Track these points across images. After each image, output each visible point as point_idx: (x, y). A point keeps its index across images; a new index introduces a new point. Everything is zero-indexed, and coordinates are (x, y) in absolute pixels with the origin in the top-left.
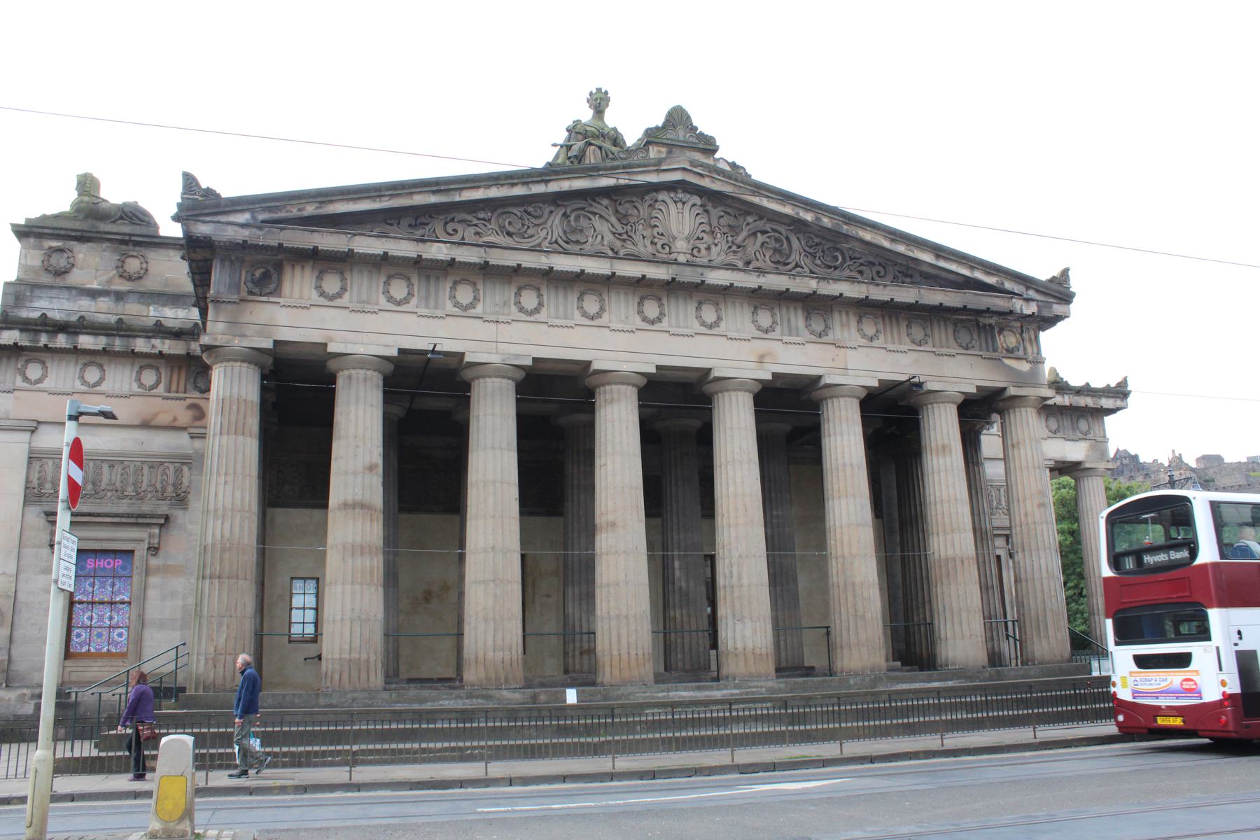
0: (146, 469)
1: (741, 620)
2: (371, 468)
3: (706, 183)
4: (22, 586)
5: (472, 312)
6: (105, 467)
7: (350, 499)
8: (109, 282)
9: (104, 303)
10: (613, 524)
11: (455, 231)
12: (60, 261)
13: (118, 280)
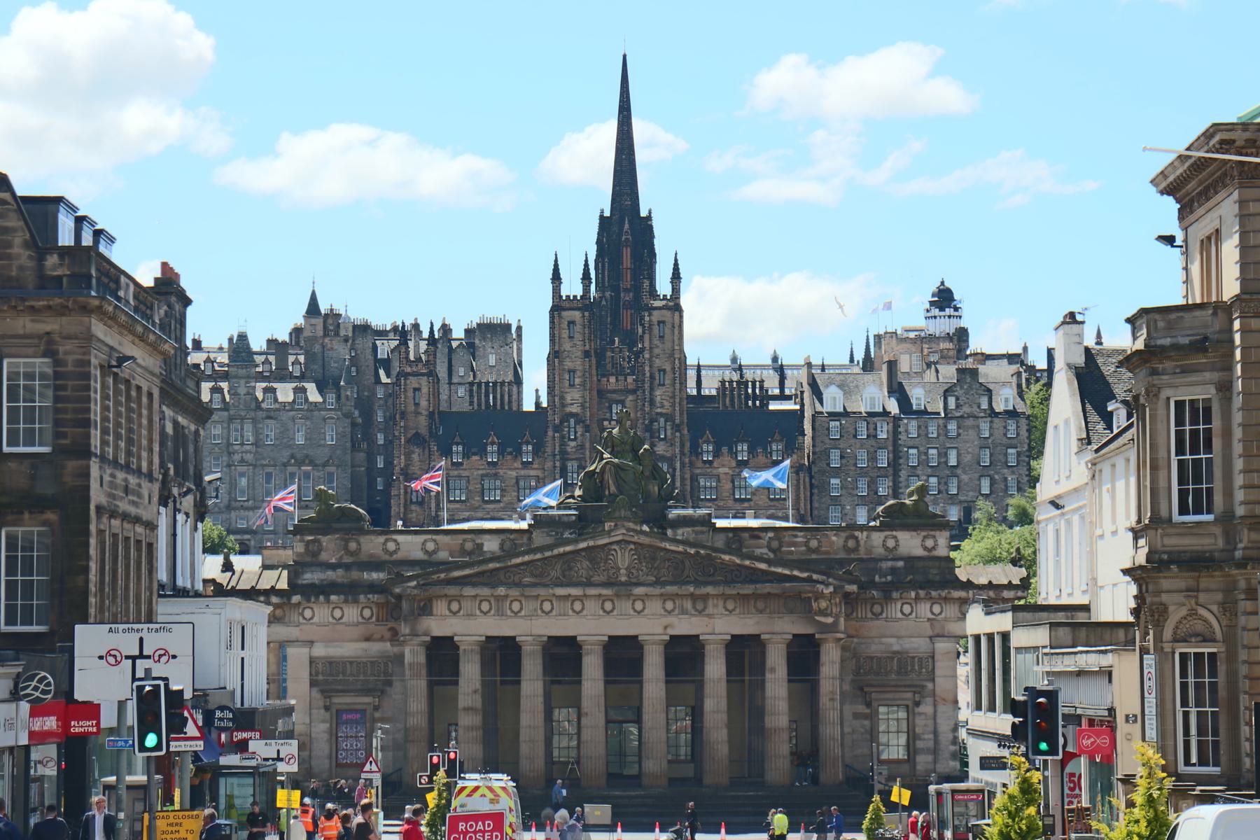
0: (369, 664)
1: (648, 759)
2: (475, 692)
3: (636, 539)
4: (313, 730)
5: (519, 614)
6: (348, 666)
7: (466, 706)
8: (341, 558)
9: (340, 572)
10: (587, 714)
11: (510, 577)
12: (314, 548)
13: (345, 557)
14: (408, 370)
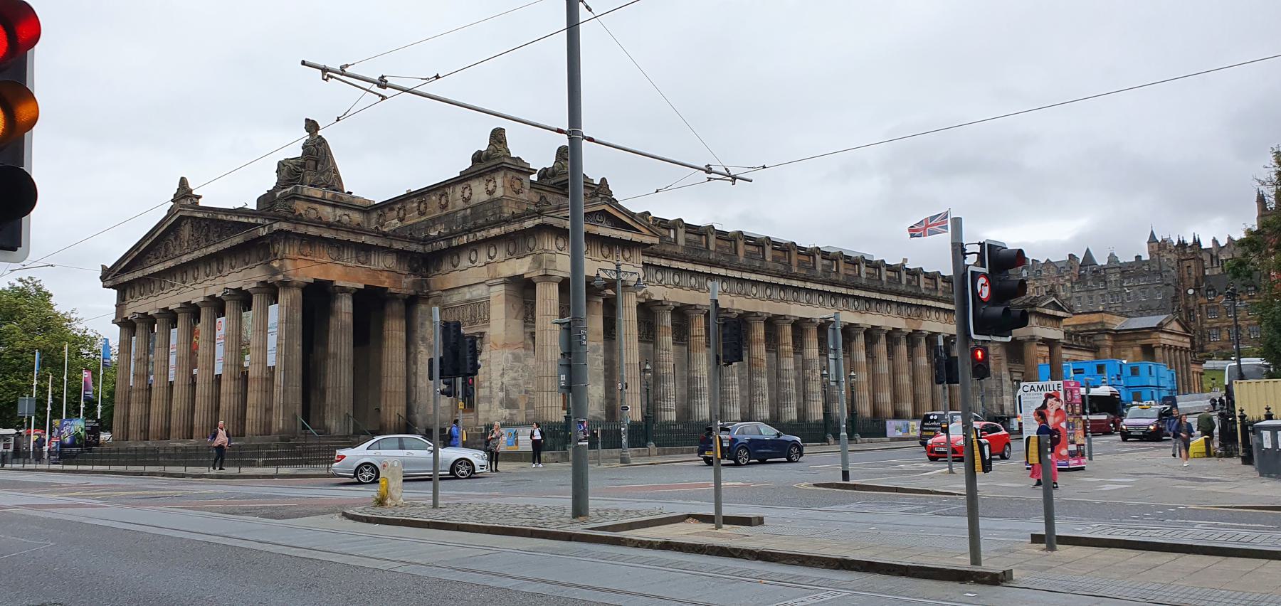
14: (1183, 258)
